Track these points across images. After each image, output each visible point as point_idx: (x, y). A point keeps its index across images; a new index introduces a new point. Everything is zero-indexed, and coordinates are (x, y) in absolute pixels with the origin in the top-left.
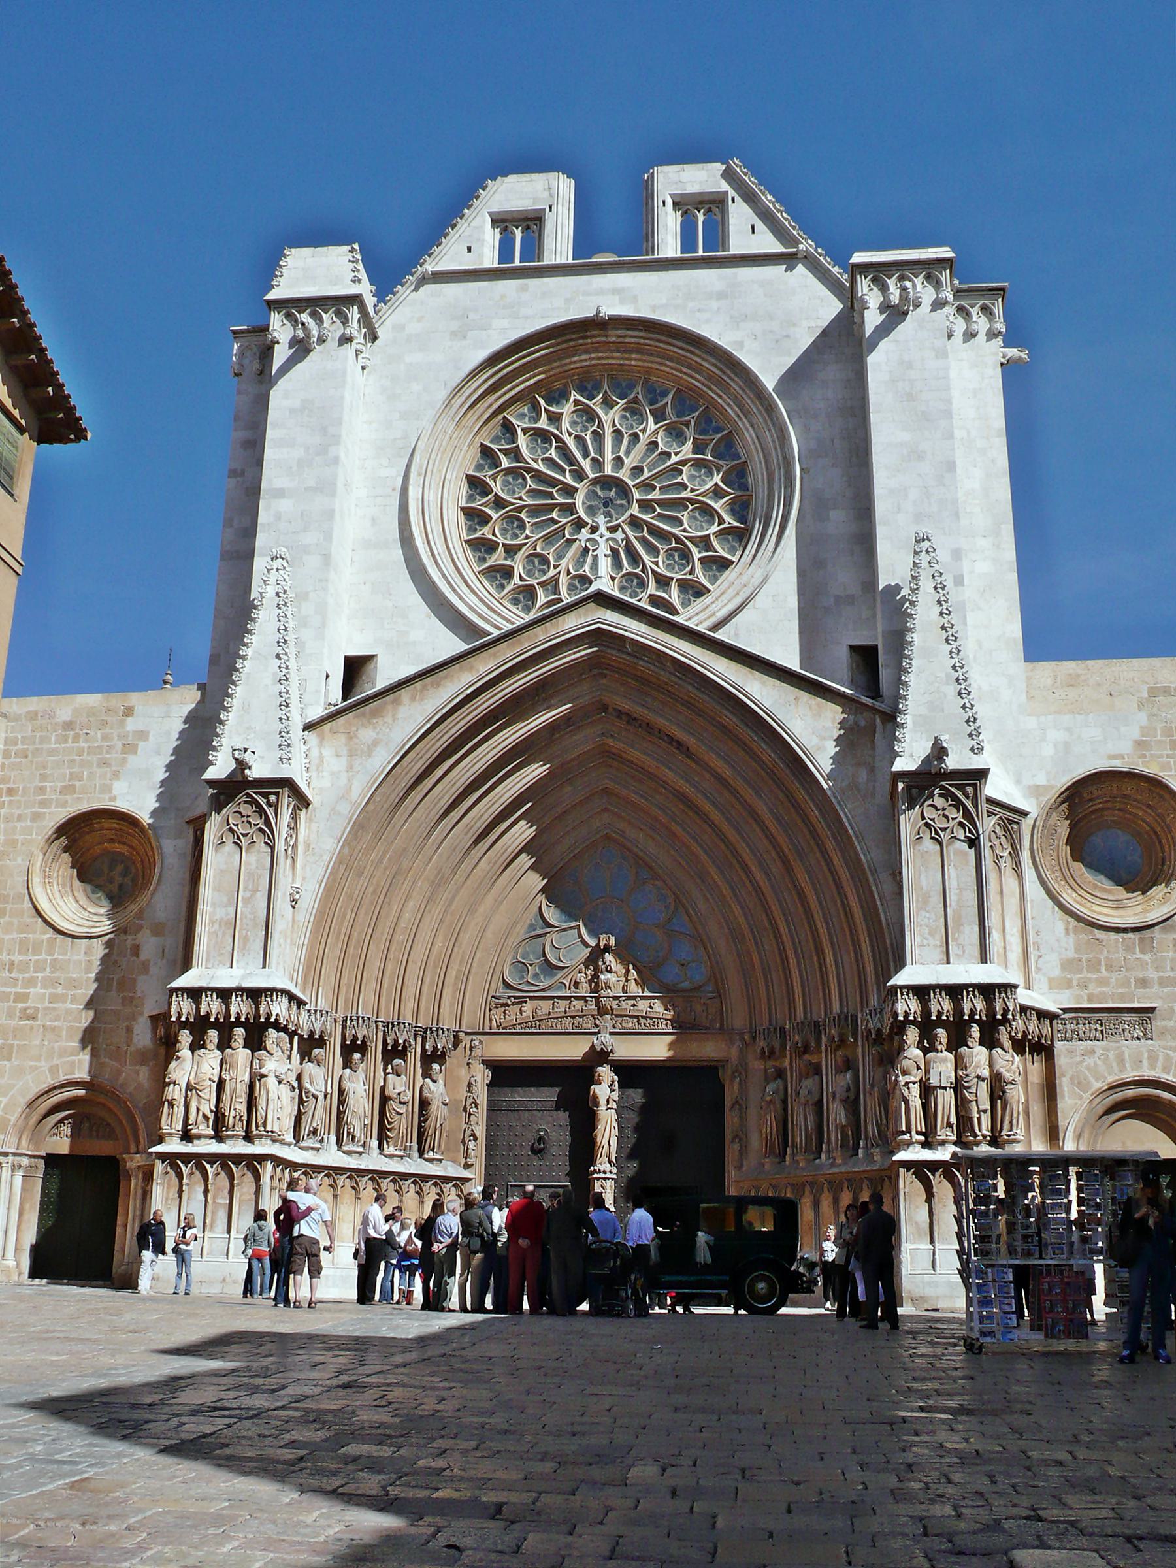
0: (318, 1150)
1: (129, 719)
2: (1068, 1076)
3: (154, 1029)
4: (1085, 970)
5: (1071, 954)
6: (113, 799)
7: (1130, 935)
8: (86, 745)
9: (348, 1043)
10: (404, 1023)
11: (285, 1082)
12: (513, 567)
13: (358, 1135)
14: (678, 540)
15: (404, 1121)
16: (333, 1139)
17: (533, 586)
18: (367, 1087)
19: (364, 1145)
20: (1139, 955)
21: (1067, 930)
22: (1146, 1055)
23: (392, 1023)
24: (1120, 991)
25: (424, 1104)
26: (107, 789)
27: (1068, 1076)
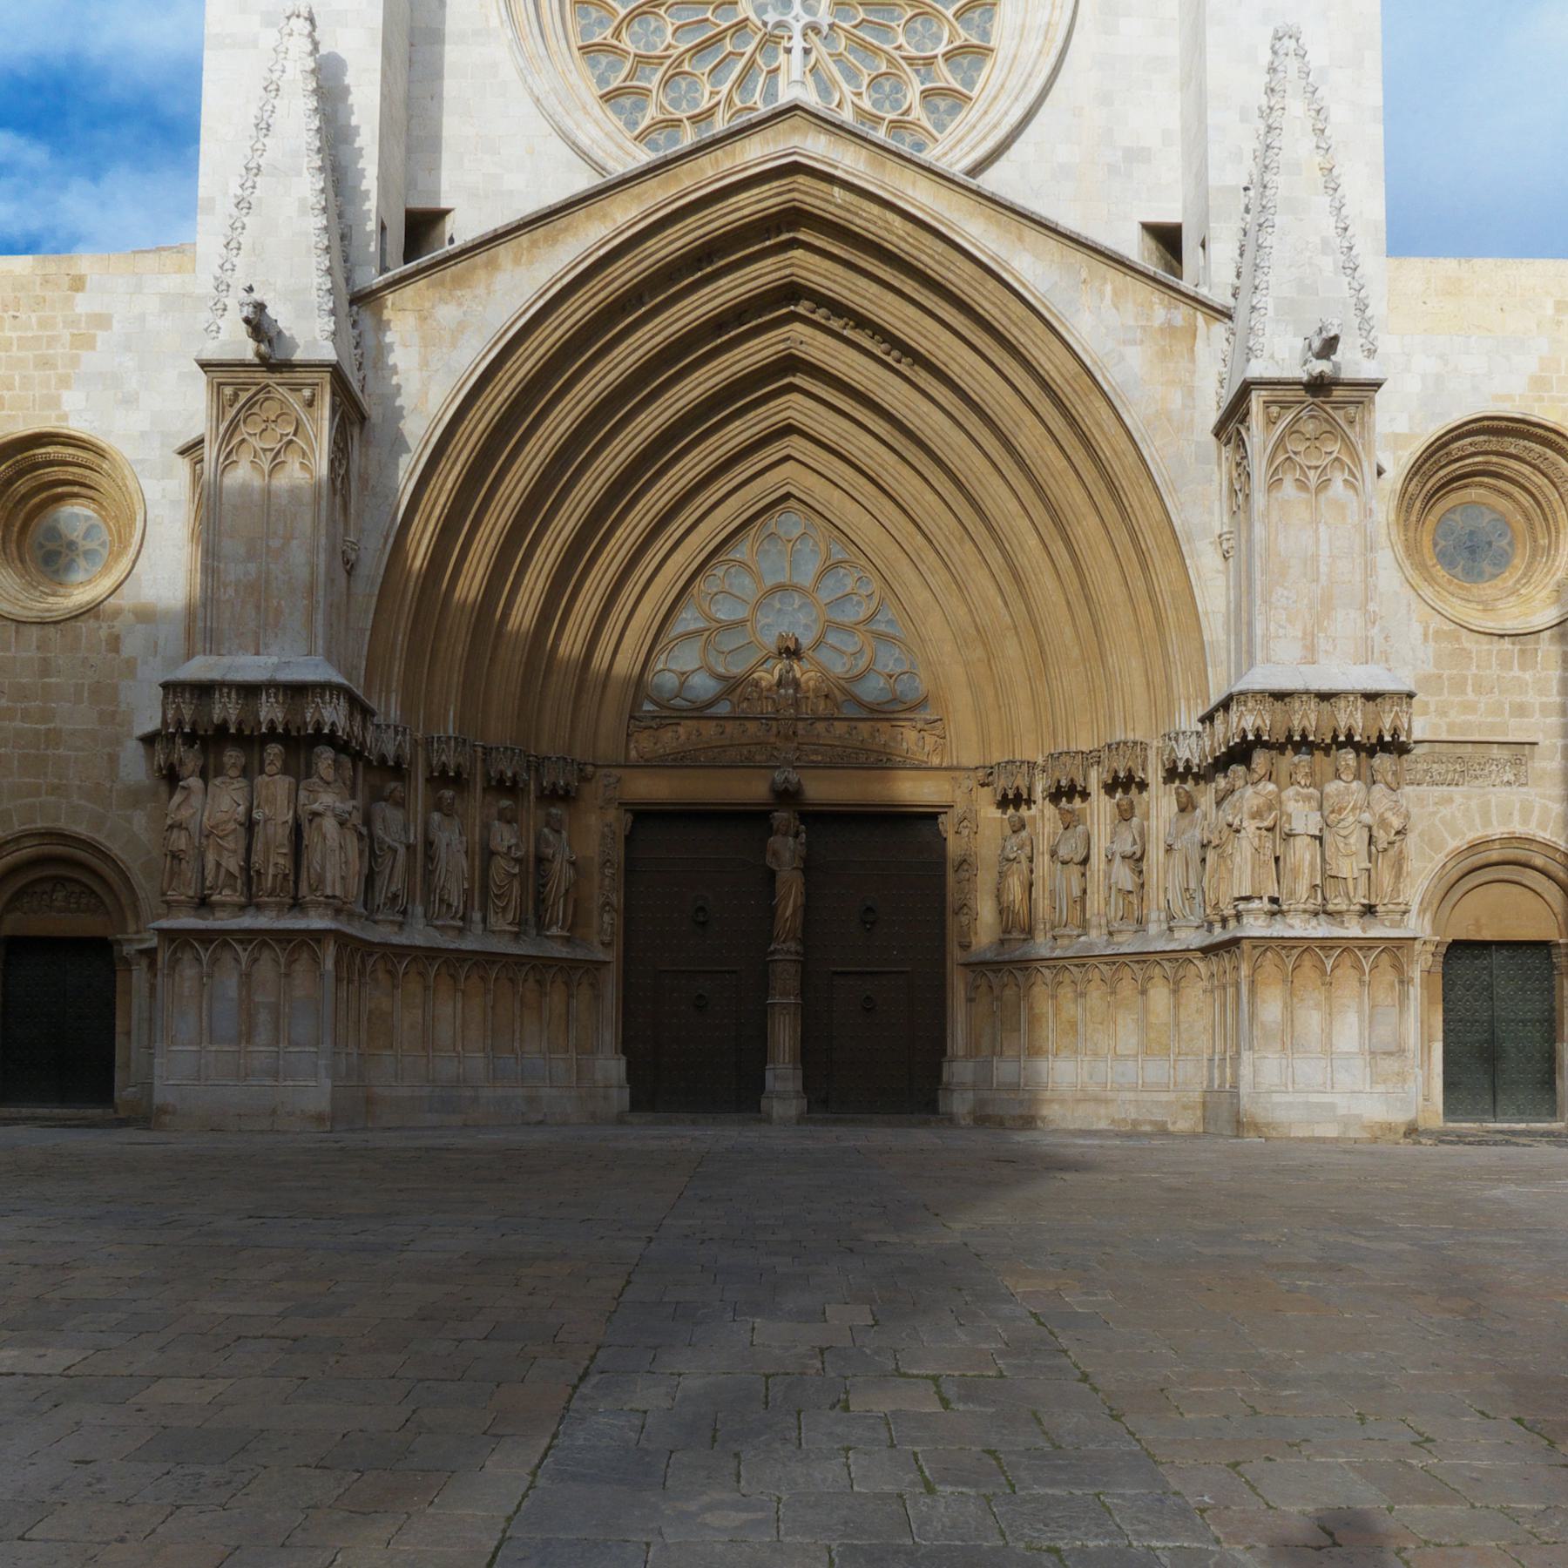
0: (401, 925)
1: (79, 296)
2: (1417, 832)
3: (150, 756)
4: (1446, 690)
5: (1430, 669)
6: (64, 417)
7: (1506, 644)
8: (14, 335)
9: (436, 774)
10: (513, 750)
11: (349, 825)
12: (651, 91)
13: (455, 904)
14: (891, 61)
15: (516, 884)
16: (419, 910)
17: (681, 121)
18: (464, 839)
19: (463, 918)
20: (1516, 672)
21: (1426, 635)
22: (1518, 806)
23: (498, 748)
24: (1489, 720)
25: (540, 860)
26: (53, 402)
27: (1417, 832)
